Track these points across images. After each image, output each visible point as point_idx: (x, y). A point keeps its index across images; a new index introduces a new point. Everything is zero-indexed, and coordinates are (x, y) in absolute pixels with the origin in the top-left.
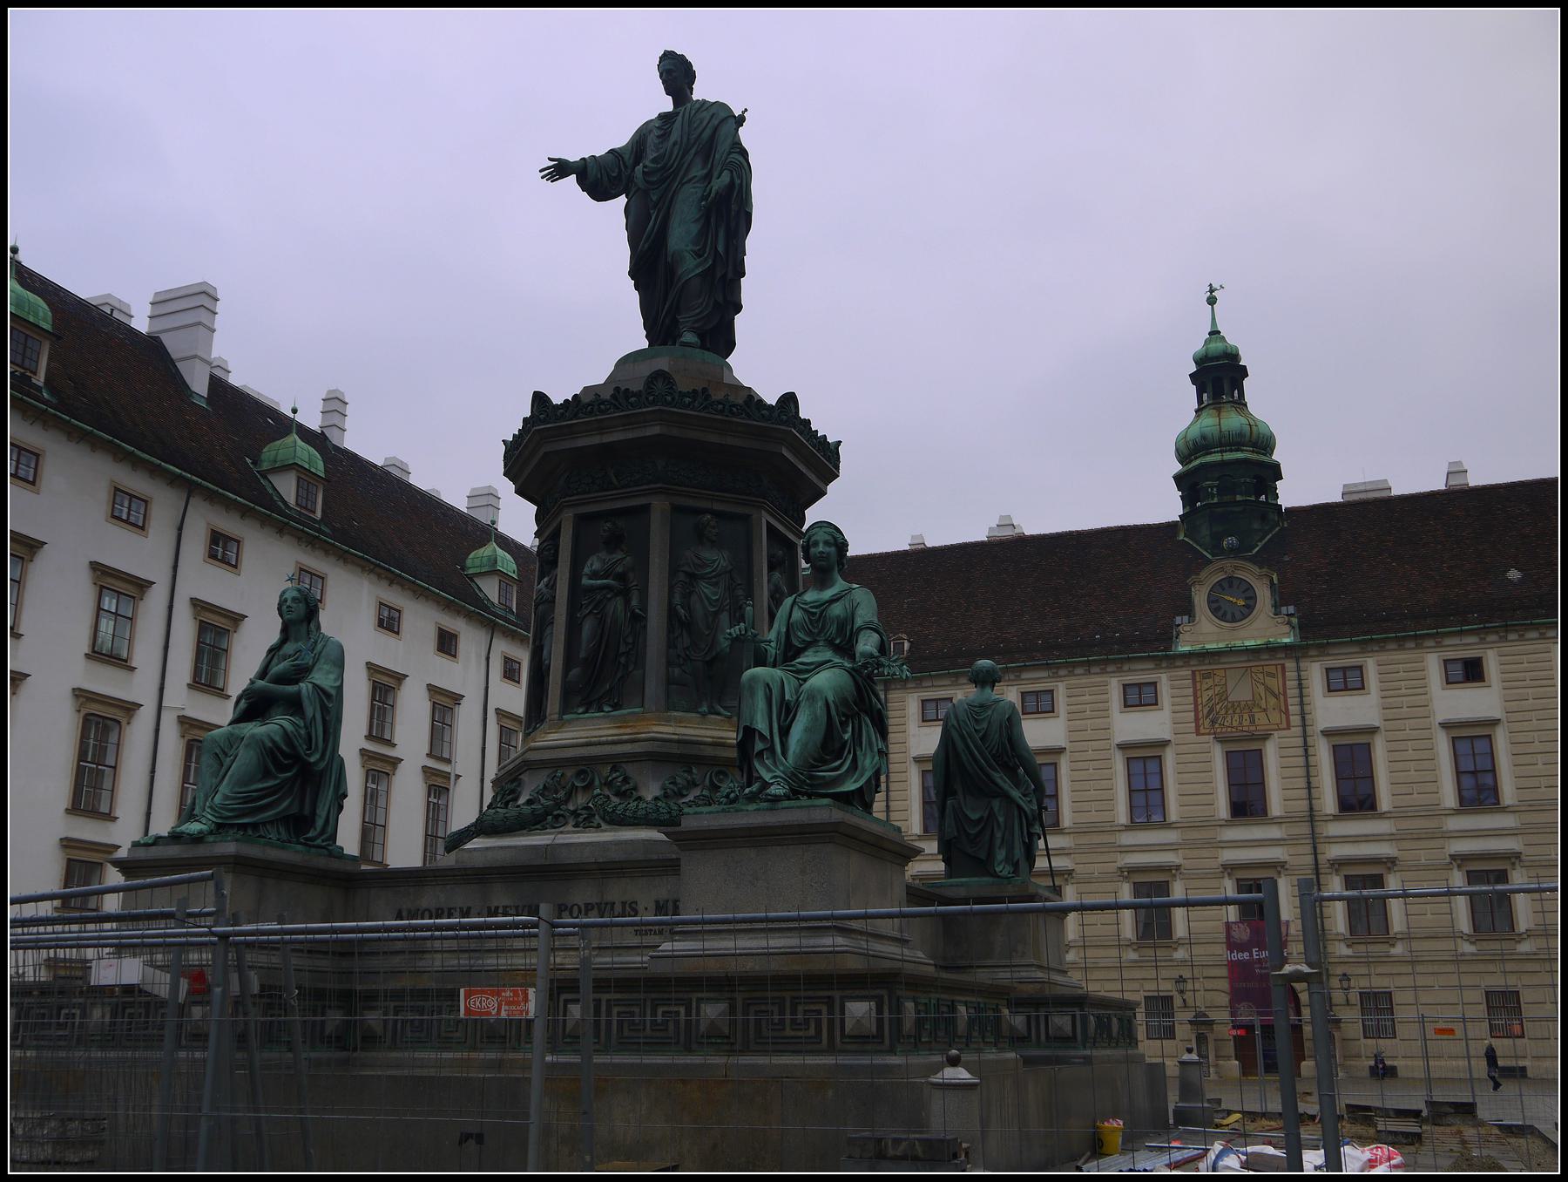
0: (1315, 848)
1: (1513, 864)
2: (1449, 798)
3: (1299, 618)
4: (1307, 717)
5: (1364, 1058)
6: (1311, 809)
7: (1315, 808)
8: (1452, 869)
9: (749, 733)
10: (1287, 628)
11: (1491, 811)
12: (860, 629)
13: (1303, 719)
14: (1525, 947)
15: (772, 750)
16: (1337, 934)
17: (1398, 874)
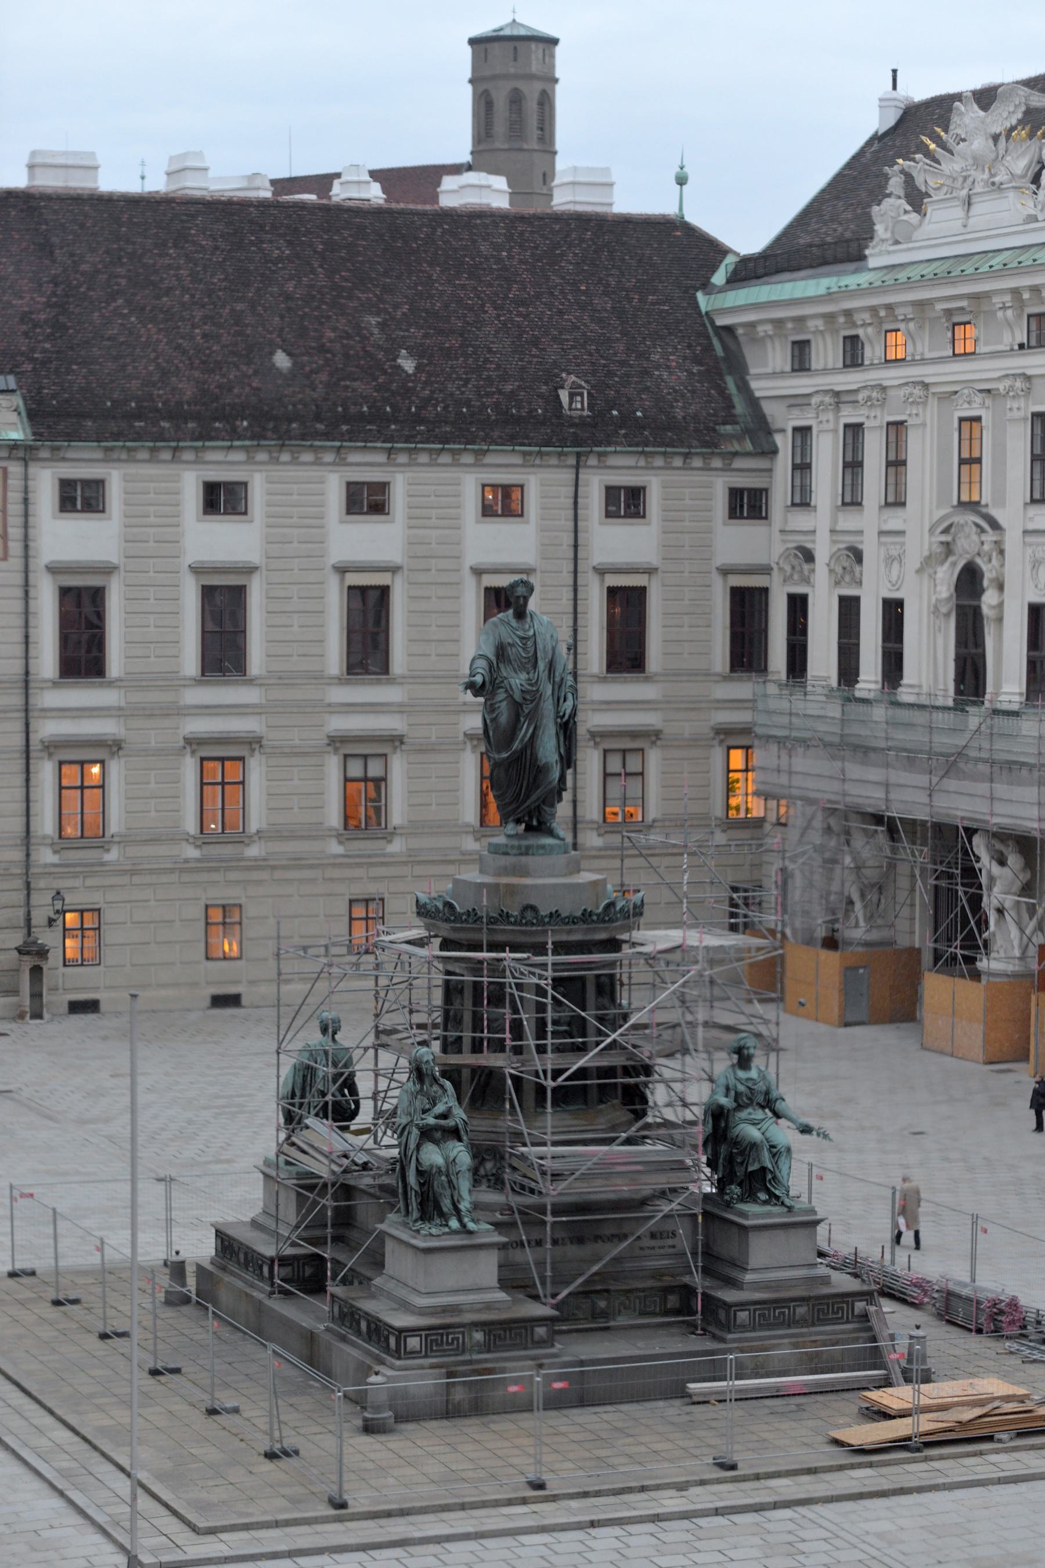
0: (27, 725)
1: (253, 750)
2: (190, 661)
3: (24, 399)
4: (31, 544)
5: (61, 991)
6: (27, 673)
7: (32, 670)
8: (184, 755)
9: (763, 1169)
10: (13, 417)
11: (236, 683)
12: (777, 1100)
13: (26, 547)
14: (254, 851)
15: (774, 1178)
16: (45, 837)
17: (123, 760)
